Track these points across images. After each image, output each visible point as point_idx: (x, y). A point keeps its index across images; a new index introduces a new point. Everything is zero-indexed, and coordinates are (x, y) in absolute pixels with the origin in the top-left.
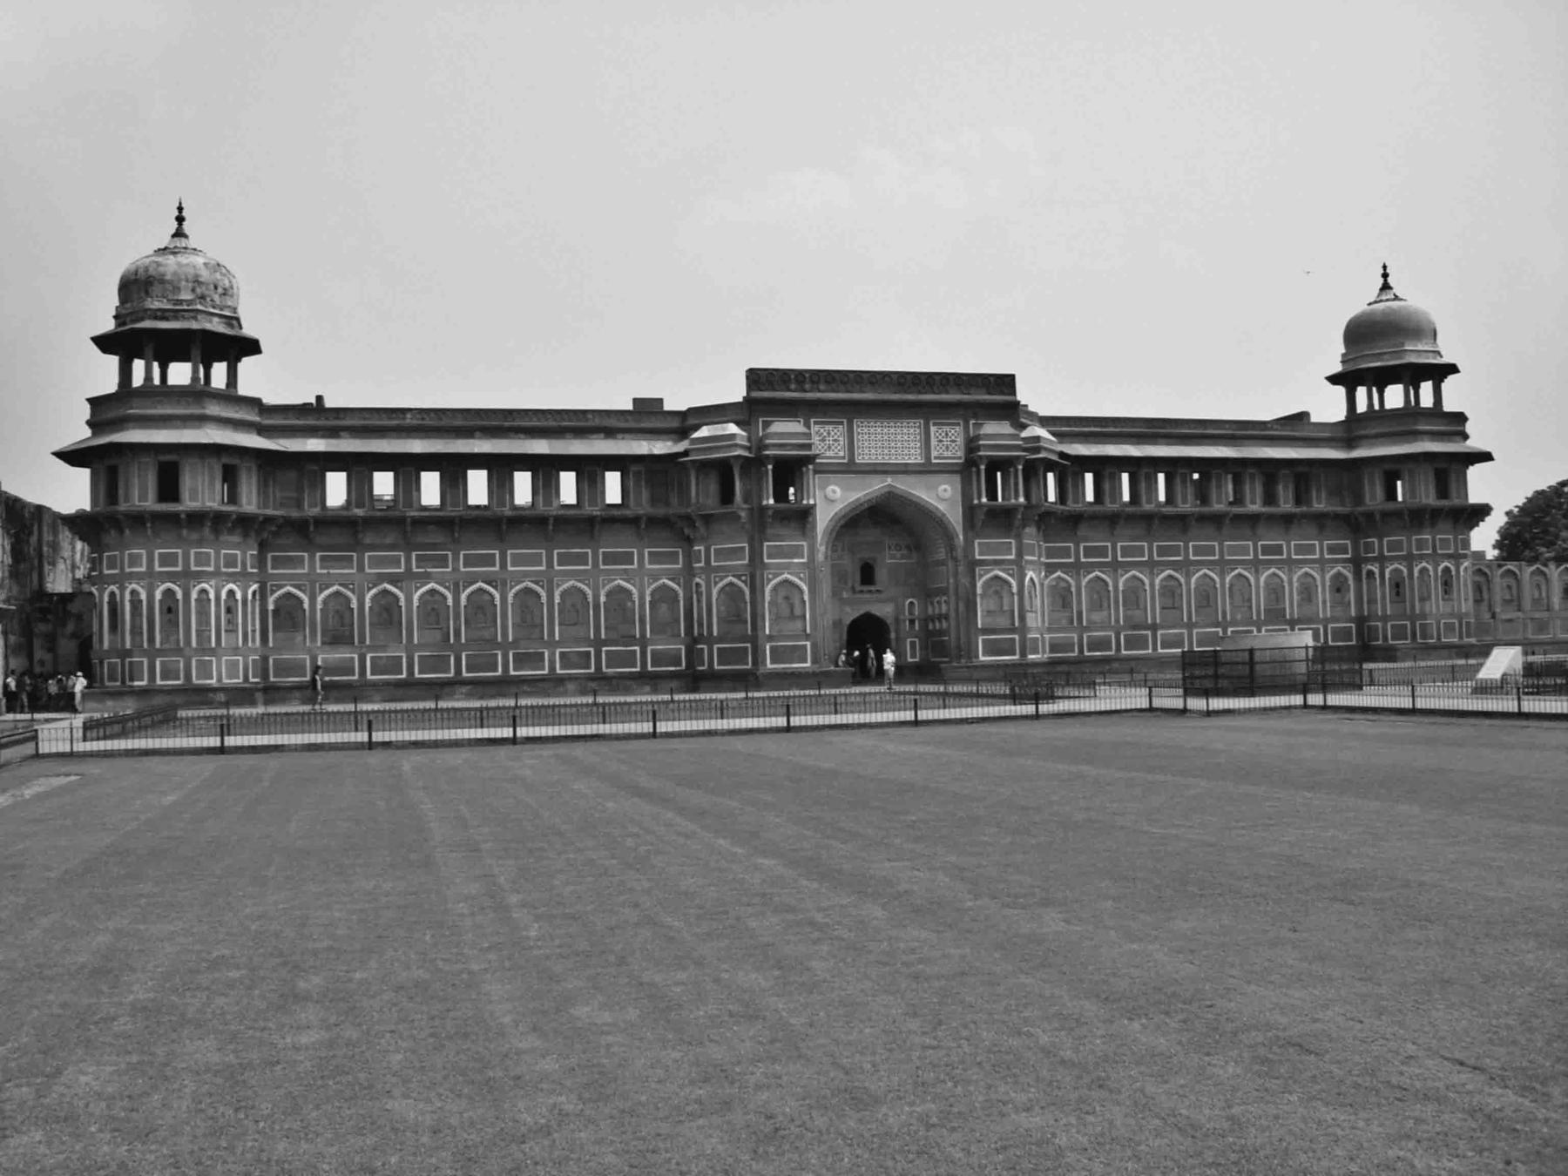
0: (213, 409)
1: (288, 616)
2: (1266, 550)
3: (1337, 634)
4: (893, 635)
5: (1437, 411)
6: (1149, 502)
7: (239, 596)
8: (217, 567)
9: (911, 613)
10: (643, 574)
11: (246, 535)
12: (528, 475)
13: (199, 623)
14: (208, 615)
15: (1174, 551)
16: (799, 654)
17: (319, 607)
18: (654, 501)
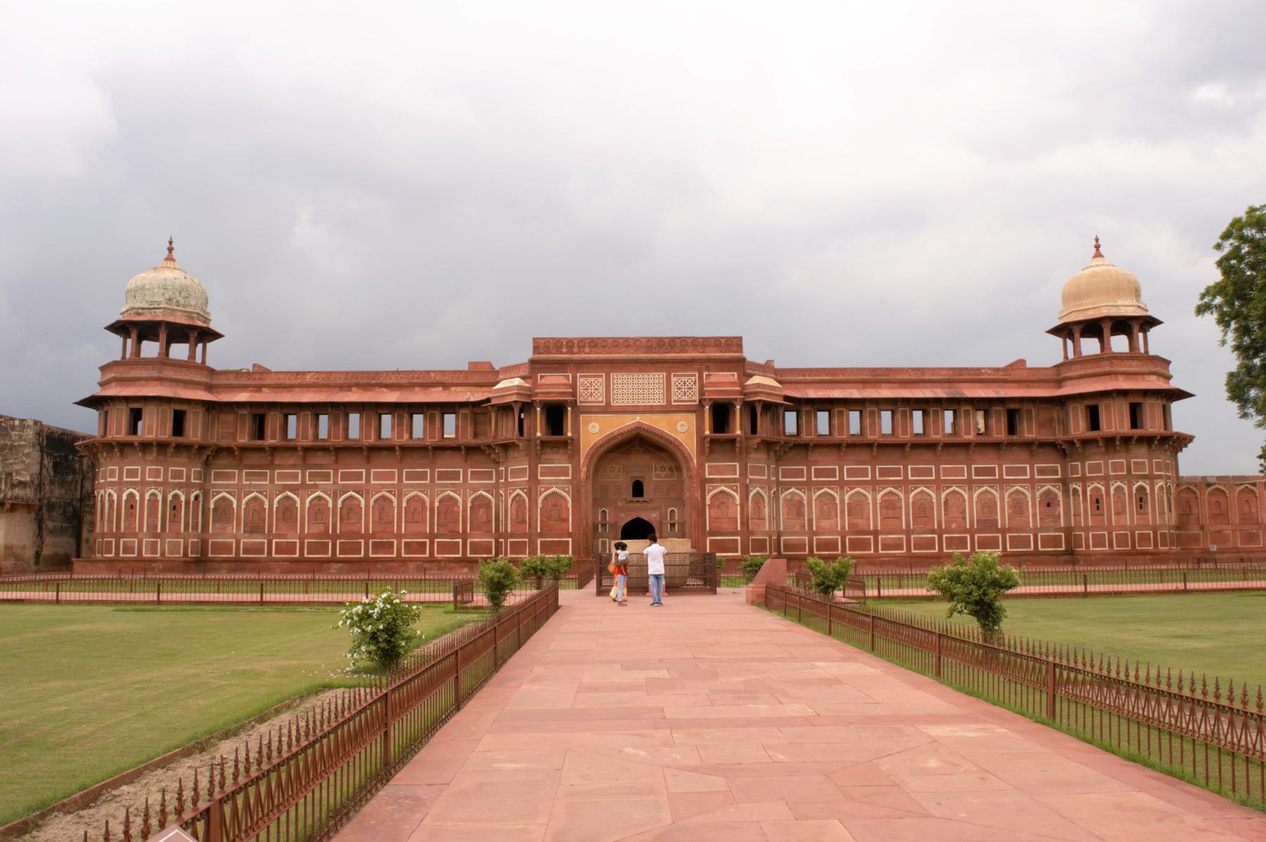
0: (169, 373)
1: (223, 510)
2: (979, 472)
3: (1046, 541)
4: (657, 535)
6: (936, 433)
7: (183, 498)
10: (464, 487)
18: (476, 435)
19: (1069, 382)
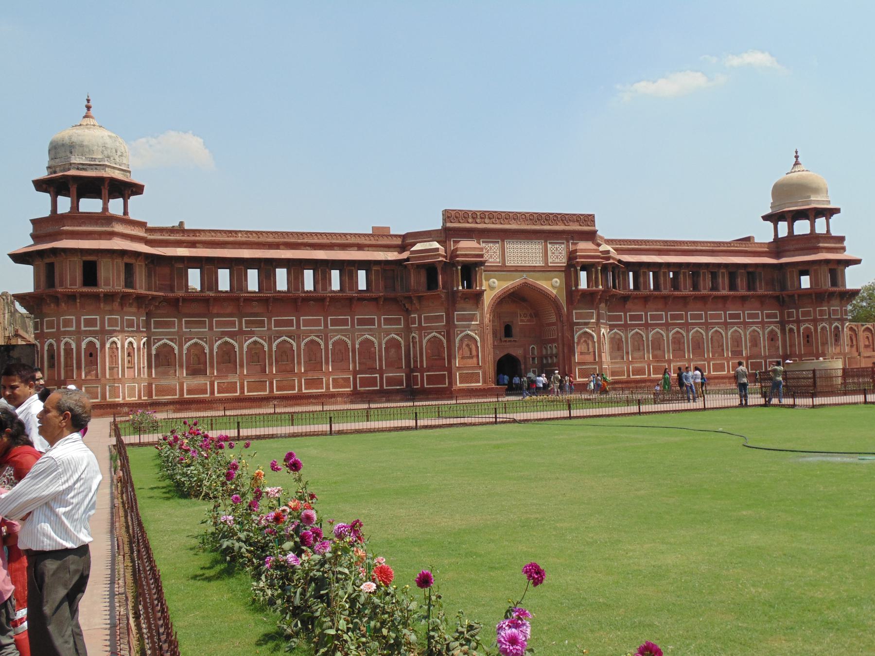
0: (118, 228)
2: (732, 316)
4: (523, 367)
5: (828, 237)
7: (135, 346)
8: (122, 327)
9: (533, 354)
10: (380, 332)
11: (139, 308)
12: (311, 271)
13: (111, 362)
14: (116, 356)
15: (680, 317)
16: (473, 377)
17: (185, 352)
18: (386, 287)
19: (788, 253)
